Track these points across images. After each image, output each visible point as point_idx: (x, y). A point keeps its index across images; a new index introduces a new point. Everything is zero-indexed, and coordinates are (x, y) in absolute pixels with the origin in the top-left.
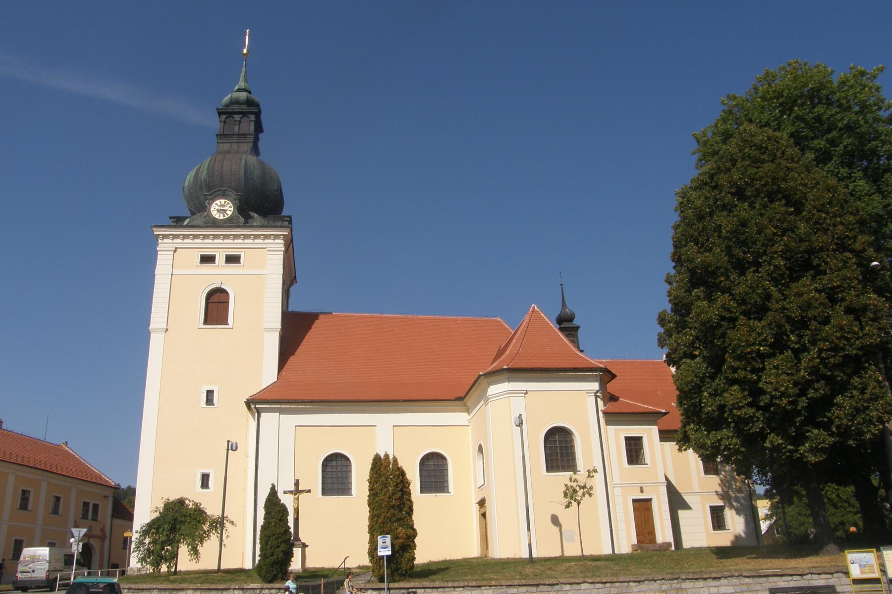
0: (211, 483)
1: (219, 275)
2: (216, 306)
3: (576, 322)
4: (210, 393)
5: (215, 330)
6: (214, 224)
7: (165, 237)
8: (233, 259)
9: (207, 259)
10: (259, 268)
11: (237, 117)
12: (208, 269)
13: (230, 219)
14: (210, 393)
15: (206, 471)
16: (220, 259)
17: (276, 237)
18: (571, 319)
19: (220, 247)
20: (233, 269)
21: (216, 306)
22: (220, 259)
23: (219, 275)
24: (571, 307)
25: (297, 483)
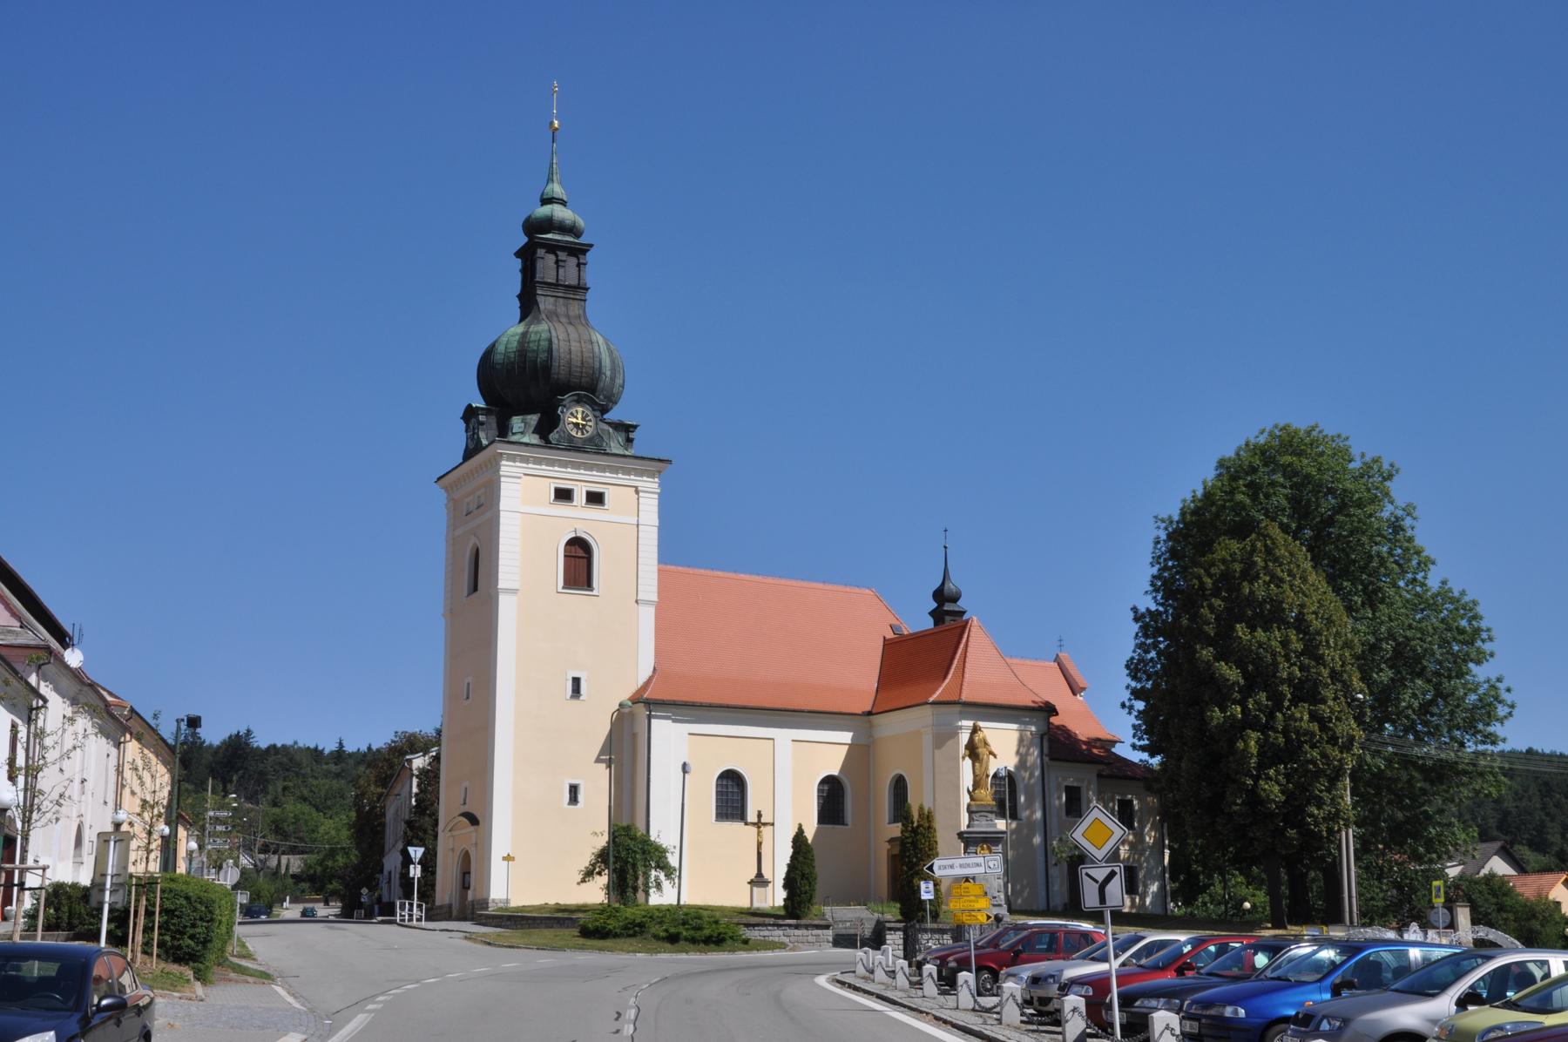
0: (581, 797)
1: (577, 519)
2: (579, 562)
3: (962, 604)
4: (576, 681)
5: (577, 598)
6: (573, 447)
7: (512, 458)
8: (595, 498)
9: (564, 495)
10: (629, 516)
11: (562, 255)
12: (562, 509)
13: (590, 440)
14: (576, 682)
15: (574, 782)
16: (580, 496)
17: (651, 474)
18: (955, 599)
19: (581, 480)
20: (594, 512)
21: (579, 562)
22: (580, 496)
23: (577, 519)
24: (956, 583)
25: (760, 815)
